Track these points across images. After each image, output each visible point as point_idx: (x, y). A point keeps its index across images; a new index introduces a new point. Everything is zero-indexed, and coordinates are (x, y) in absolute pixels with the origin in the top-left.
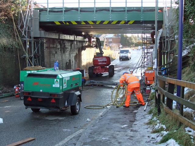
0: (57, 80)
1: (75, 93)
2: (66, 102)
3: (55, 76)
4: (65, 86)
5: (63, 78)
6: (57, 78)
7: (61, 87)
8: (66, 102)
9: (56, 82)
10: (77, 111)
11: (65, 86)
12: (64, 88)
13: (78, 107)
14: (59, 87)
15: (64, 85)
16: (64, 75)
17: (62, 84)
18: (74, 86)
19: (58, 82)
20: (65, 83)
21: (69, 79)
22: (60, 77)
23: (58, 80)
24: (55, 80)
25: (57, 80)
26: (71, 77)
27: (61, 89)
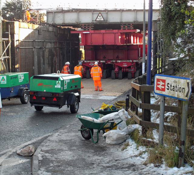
0: (58, 82)
2: (66, 101)
3: (57, 79)
4: (66, 87)
7: (62, 87)
9: (58, 83)
11: (66, 87)
12: (64, 89)
14: (60, 87)
15: (65, 86)
16: (65, 78)
18: (74, 88)
19: (59, 83)
20: (65, 85)
21: (69, 81)
22: (62, 79)
23: (60, 82)
24: (57, 82)
25: (58, 82)
26: (70, 79)
27: (62, 89)
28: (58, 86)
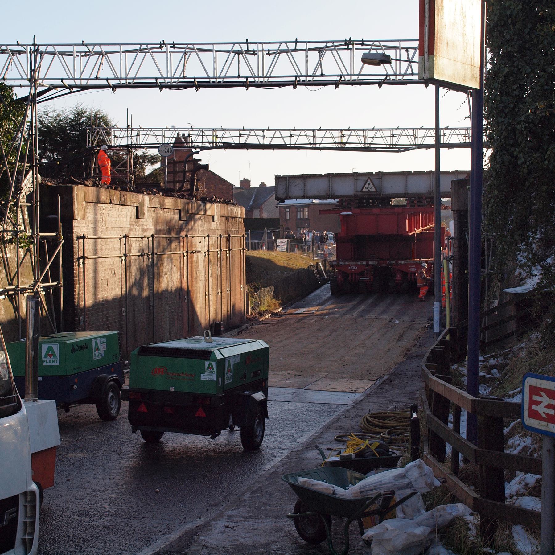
2: (231, 417)
6: (211, 357)
7: (220, 379)
8: (231, 417)
11: (229, 378)
12: (226, 382)
20: (229, 371)
26: (242, 355)
27: (220, 385)
28: (210, 376)
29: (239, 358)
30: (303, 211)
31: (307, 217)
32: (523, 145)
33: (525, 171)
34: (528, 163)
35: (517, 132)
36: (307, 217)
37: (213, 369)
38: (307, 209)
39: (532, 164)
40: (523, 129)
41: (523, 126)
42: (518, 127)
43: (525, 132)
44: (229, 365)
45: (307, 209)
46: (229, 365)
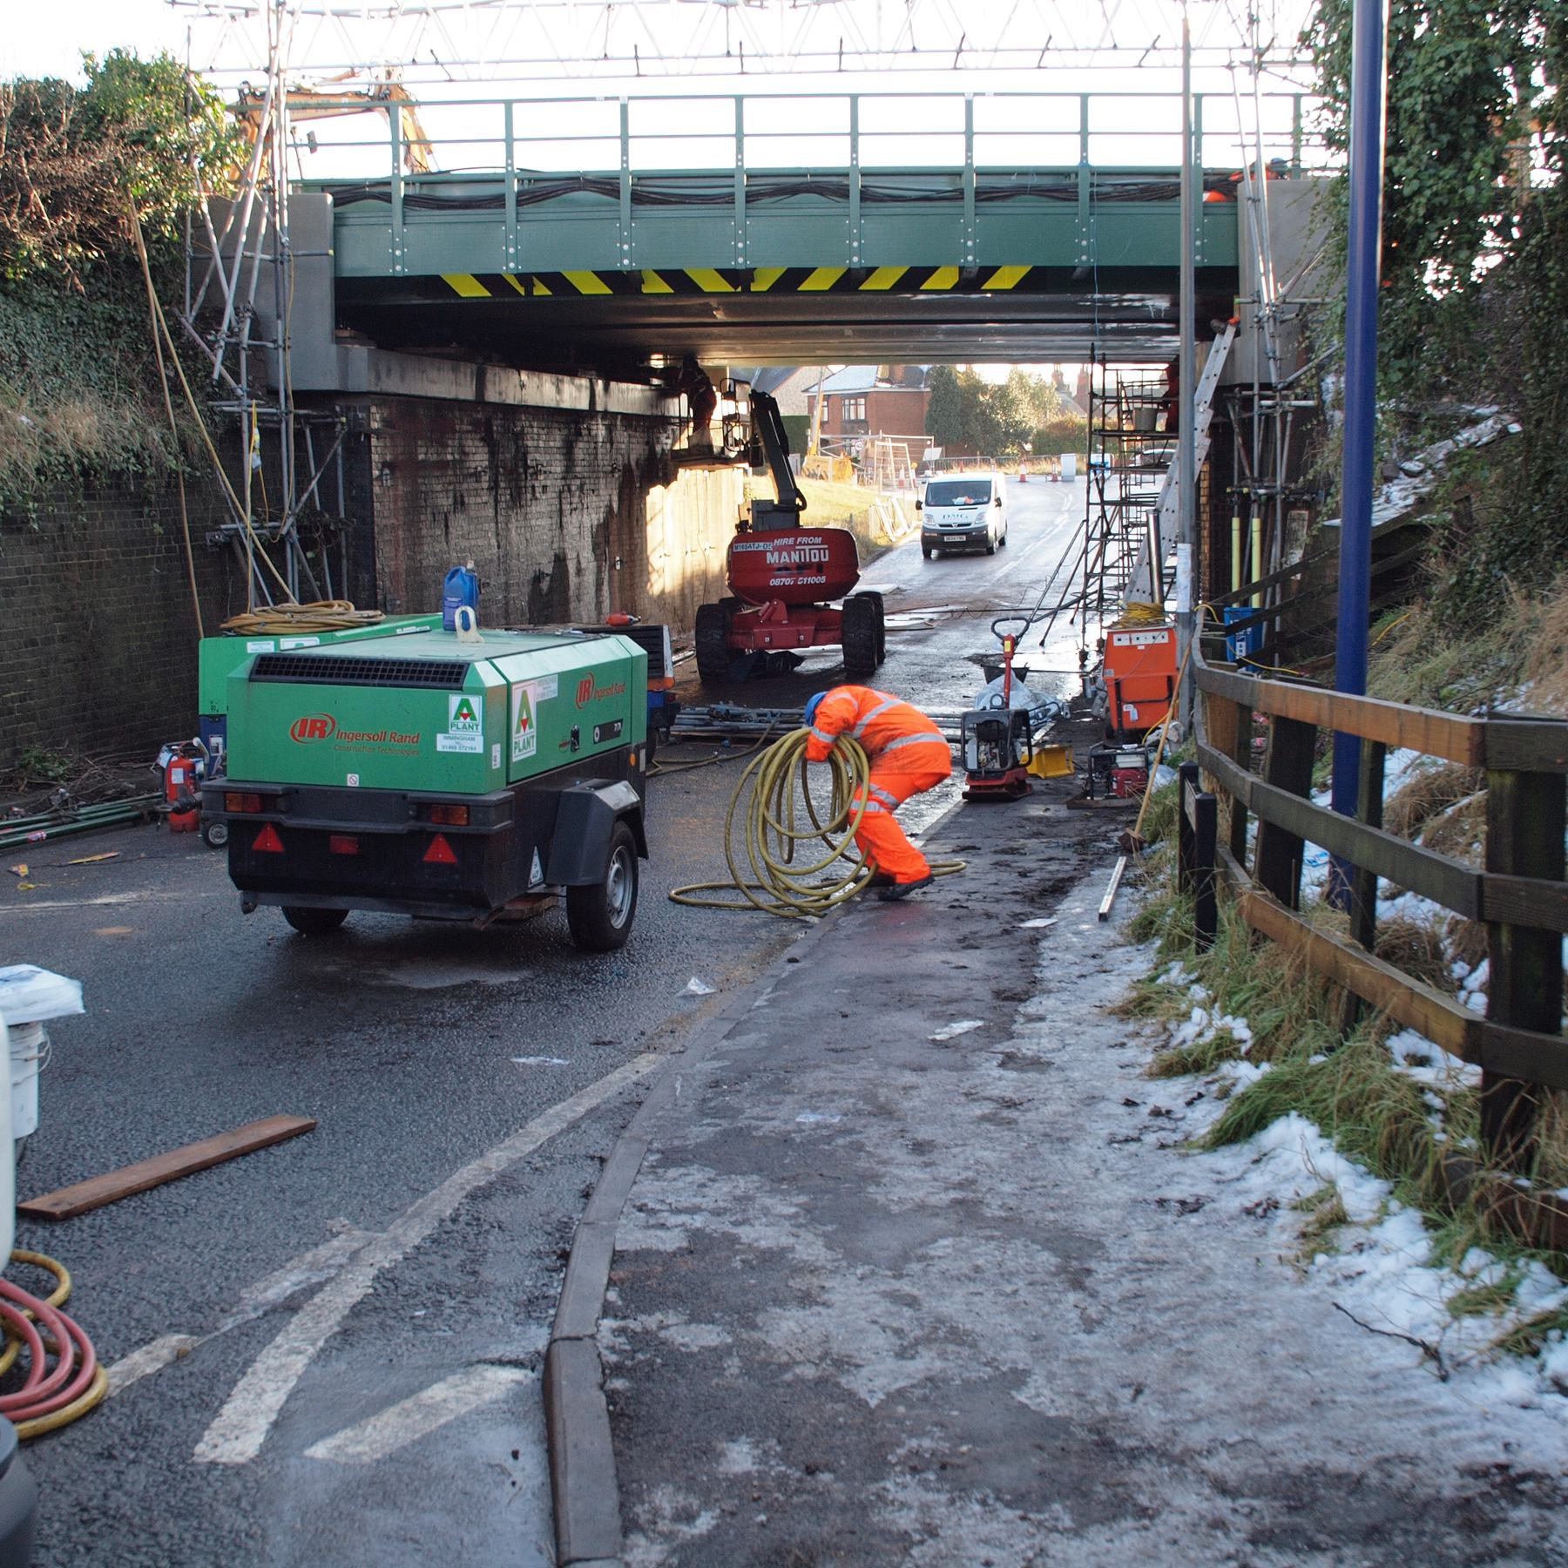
0: (465, 703)
1: (601, 794)
2: (536, 860)
3: (451, 675)
4: (525, 745)
5: (509, 685)
6: (467, 683)
7: (497, 750)
8: (536, 860)
10: (618, 922)
12: (516, 757)
13: (619, 896)
14: (480, 750)
15: (519, 737)
17: (500, 724)
18: (590, 746)
19: (470, 715)
20: (524, 723)
22: (491, 679)
23: (476, 703)
24: (455, 700)
25: (465, 703)
27: (497, 763)
29: (554, 686)
30: (856, 404)
31: (862, 417)
32: (1415, 148)
33: (1422, 212)
34: (1428, 193)
35: (1402, 116)
36: (862, 417)
37: (474, 719)
38: (862, 401)
39: (1436, 194)
40: (1419, 108)
41: (1420, 100)
42: (1407, 103)
43: (1422, 116)
44: (525, 704)
45: (862, 401)
46: (525, 704)
